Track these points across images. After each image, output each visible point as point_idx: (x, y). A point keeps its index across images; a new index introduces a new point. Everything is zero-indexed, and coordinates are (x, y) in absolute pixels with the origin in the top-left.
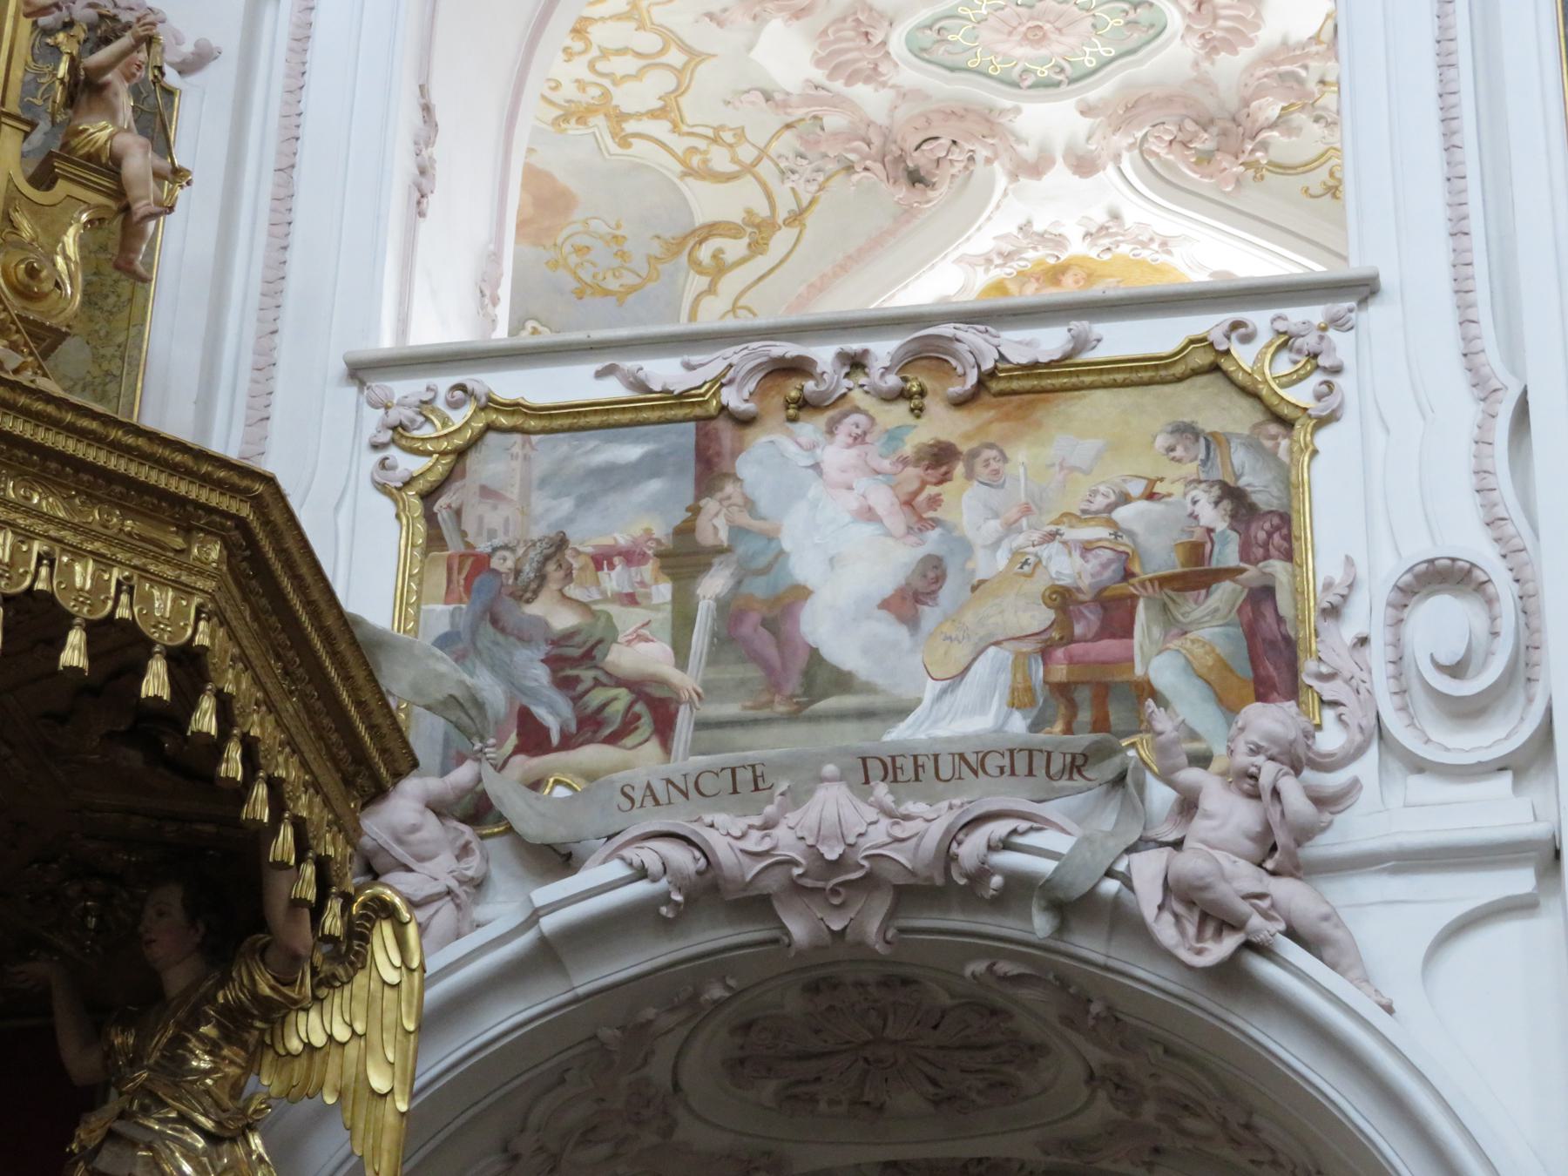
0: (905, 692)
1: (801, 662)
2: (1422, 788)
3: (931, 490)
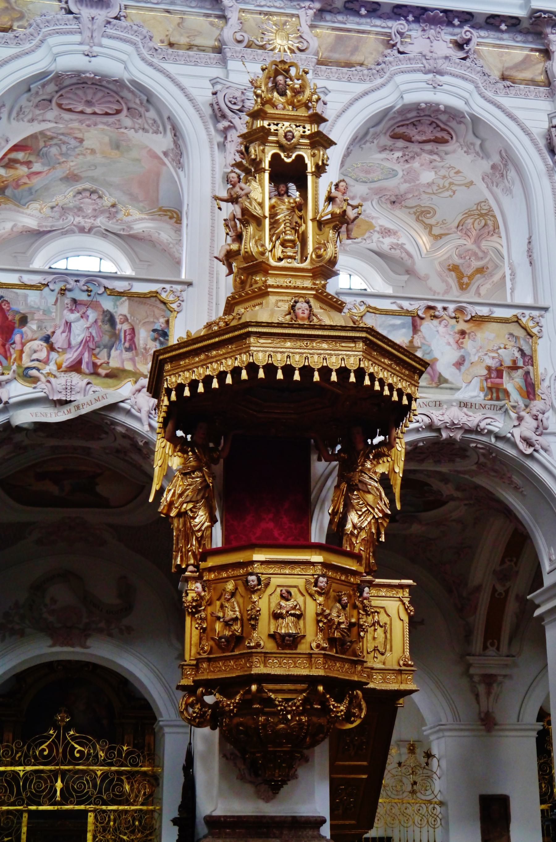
0: (459, 385)
1: (437, 375)
3: (461, 340)
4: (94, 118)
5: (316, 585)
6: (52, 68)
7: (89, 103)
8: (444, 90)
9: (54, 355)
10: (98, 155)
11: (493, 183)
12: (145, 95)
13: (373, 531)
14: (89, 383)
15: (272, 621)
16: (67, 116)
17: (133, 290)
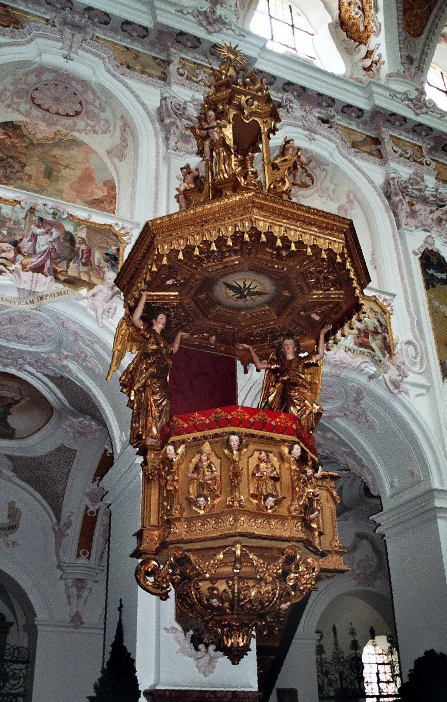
4: (56, 117)
6: (37, 60)
7: (56, 100)
9: (20, 257)
10: (33, 182)
16: (36, 112)
17: (91, 220)
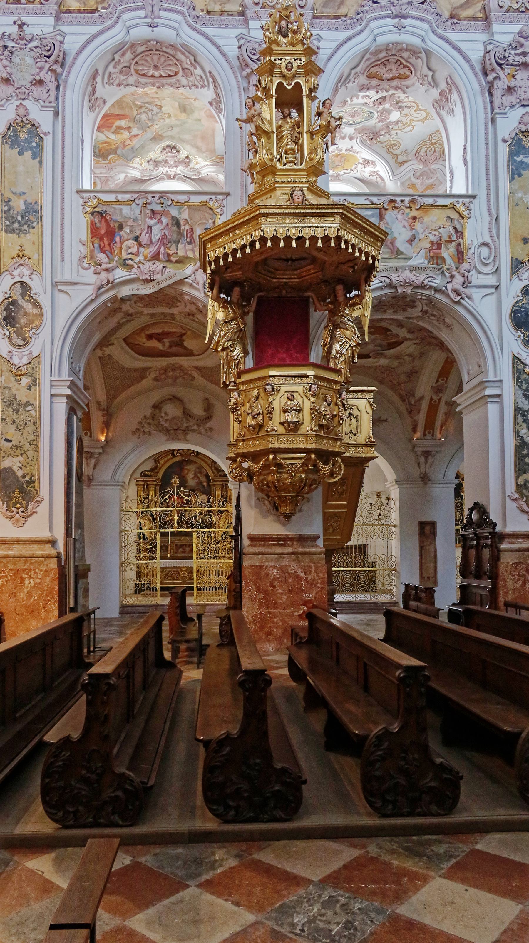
0: (411, 256)
1: (396, 250)
2: (480, 276)
5: (310, 391)
8: (406, 31)
9: (142, 250)
11: (440, 107)
12: (193, 56)
13: (350, 355)
14: (164, 267)
15: (282, 414)
